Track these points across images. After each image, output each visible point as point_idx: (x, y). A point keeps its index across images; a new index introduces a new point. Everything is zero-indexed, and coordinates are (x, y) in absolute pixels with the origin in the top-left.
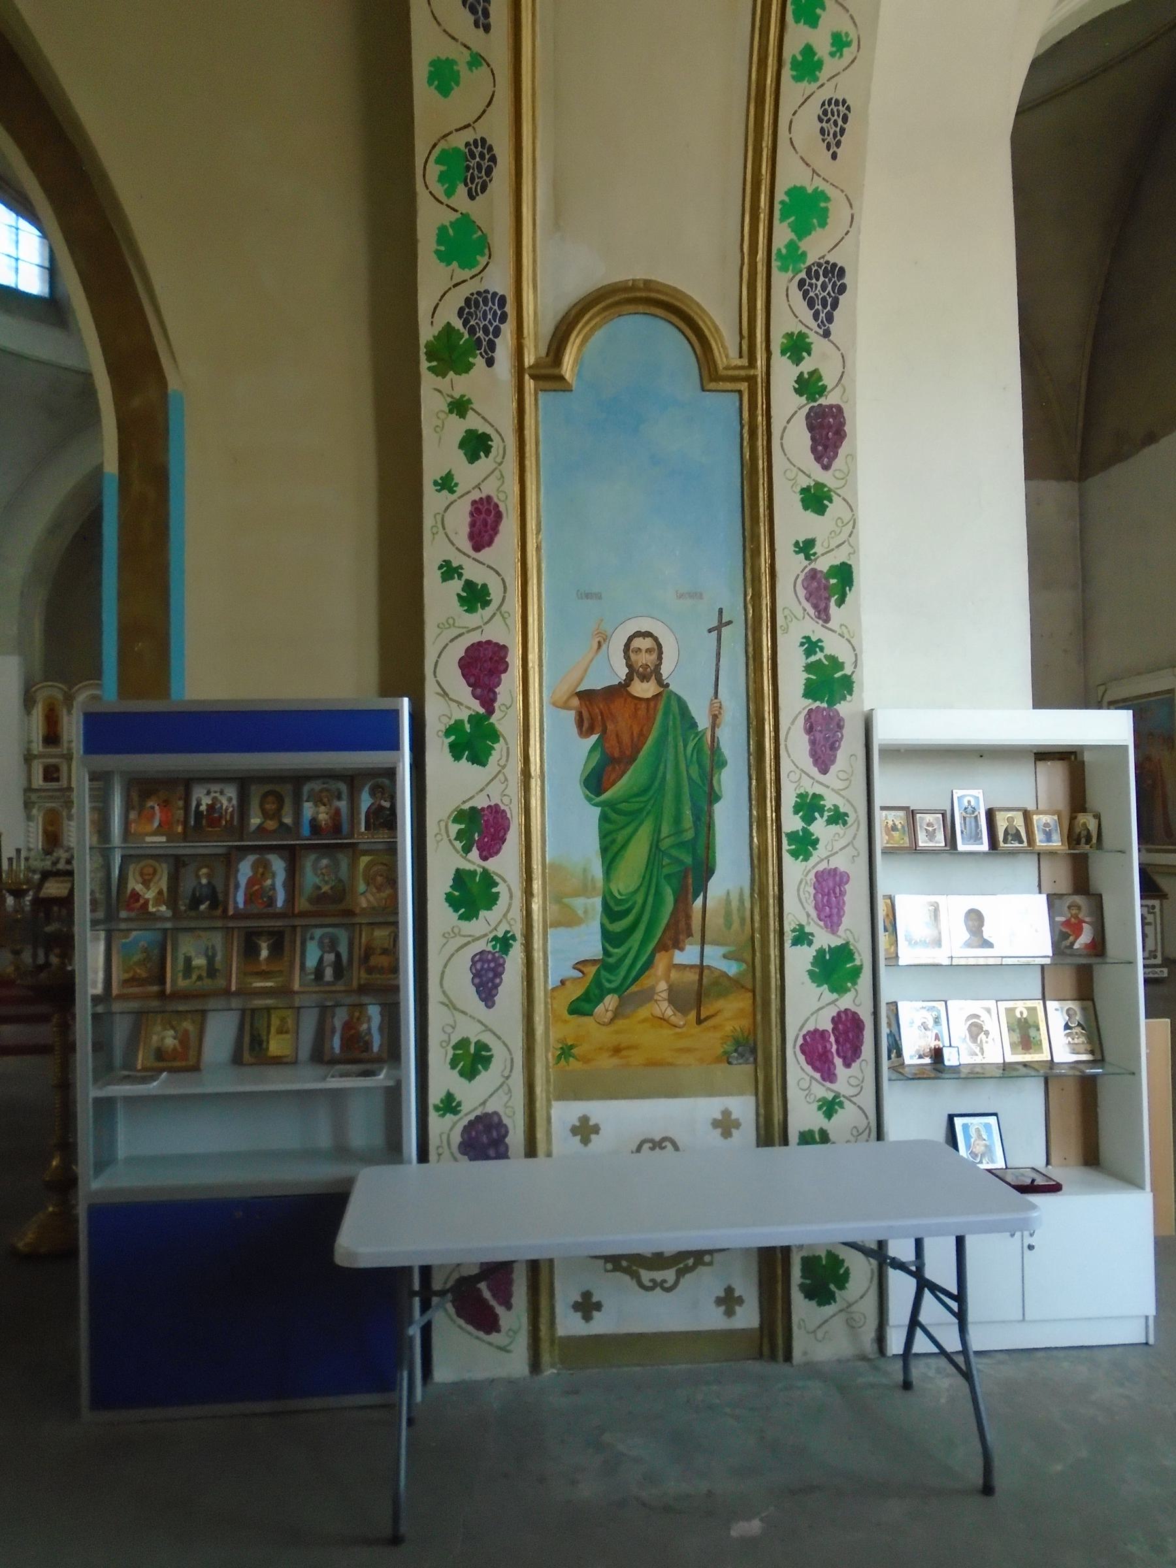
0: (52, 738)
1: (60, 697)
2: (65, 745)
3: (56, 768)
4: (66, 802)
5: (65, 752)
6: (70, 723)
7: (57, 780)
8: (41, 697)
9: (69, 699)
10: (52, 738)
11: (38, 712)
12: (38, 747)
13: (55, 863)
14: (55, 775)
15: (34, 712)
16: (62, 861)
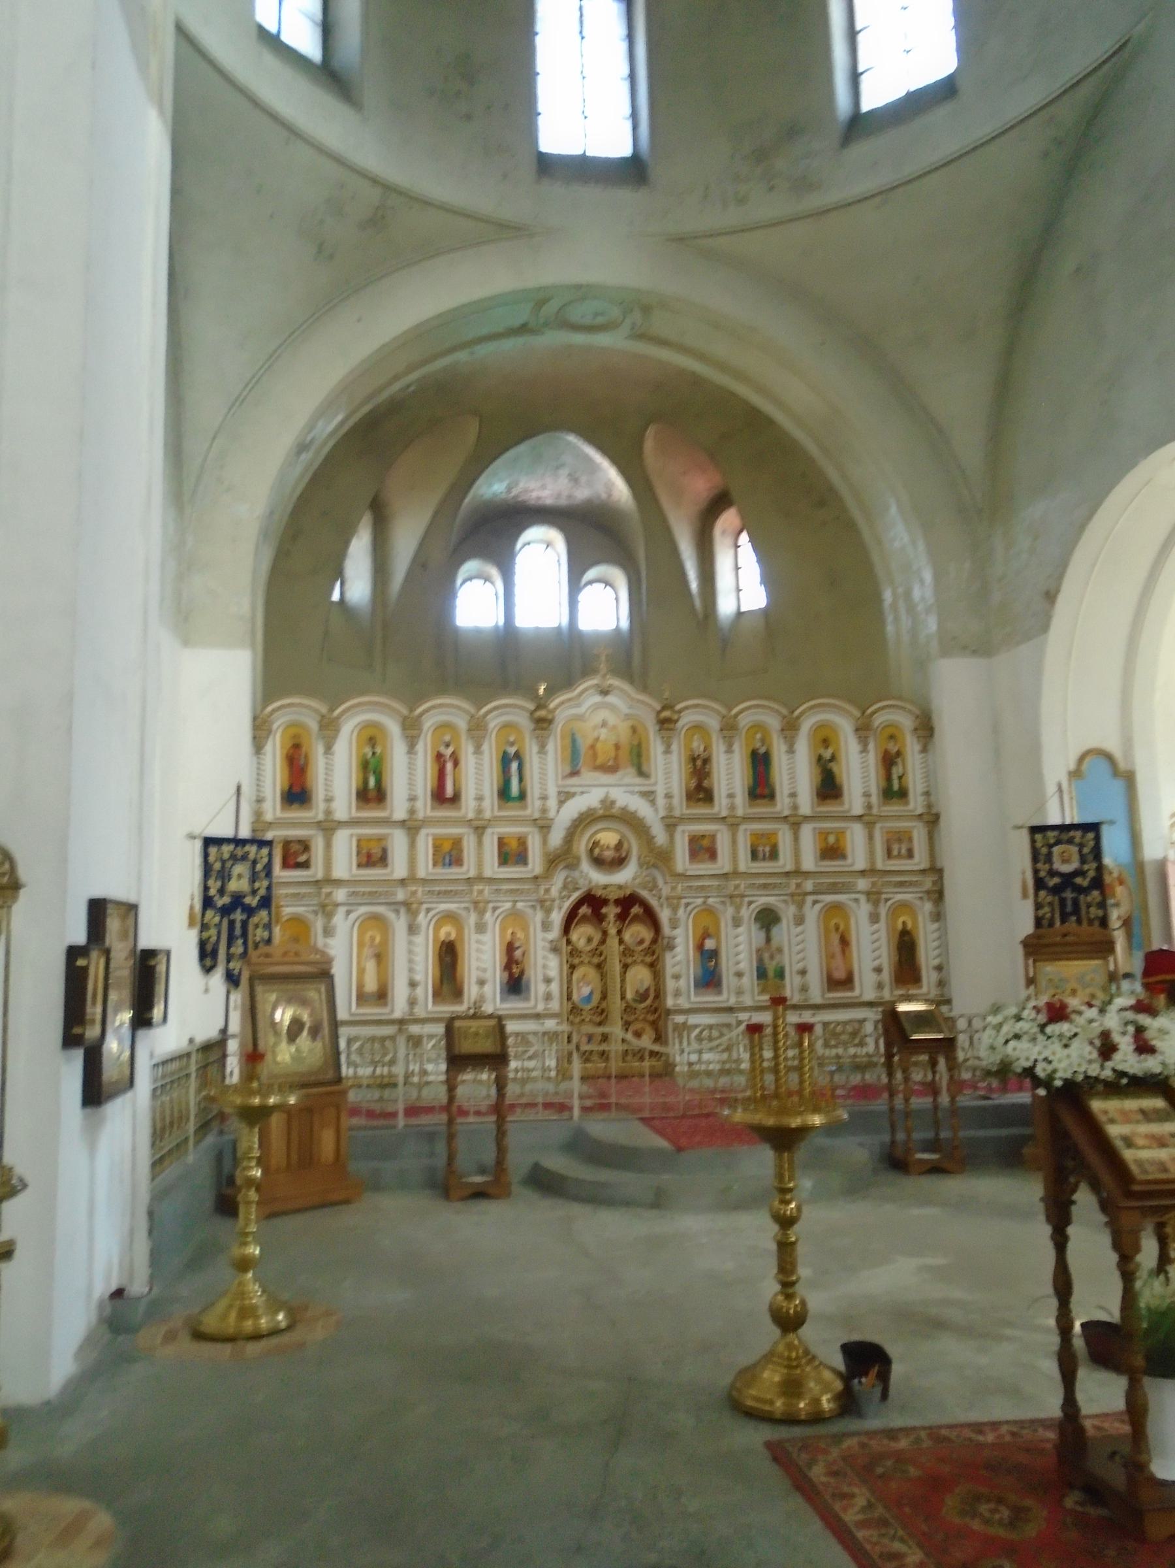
0: (297, 794)
1: (313, 725)
2: (322, 806)
3: (305, 846)
4: (323, 906)
5: (321, 817)
6: (329, 769)
7: (305, 865)
8: (279, 723)
9: (329, 728)
10: (297, 794)
11: (275, 749)
12: (273, 809)
13: (1107, 1049)
14: (302, 859)
15: (268, 748)
16: (1125, 1044)
